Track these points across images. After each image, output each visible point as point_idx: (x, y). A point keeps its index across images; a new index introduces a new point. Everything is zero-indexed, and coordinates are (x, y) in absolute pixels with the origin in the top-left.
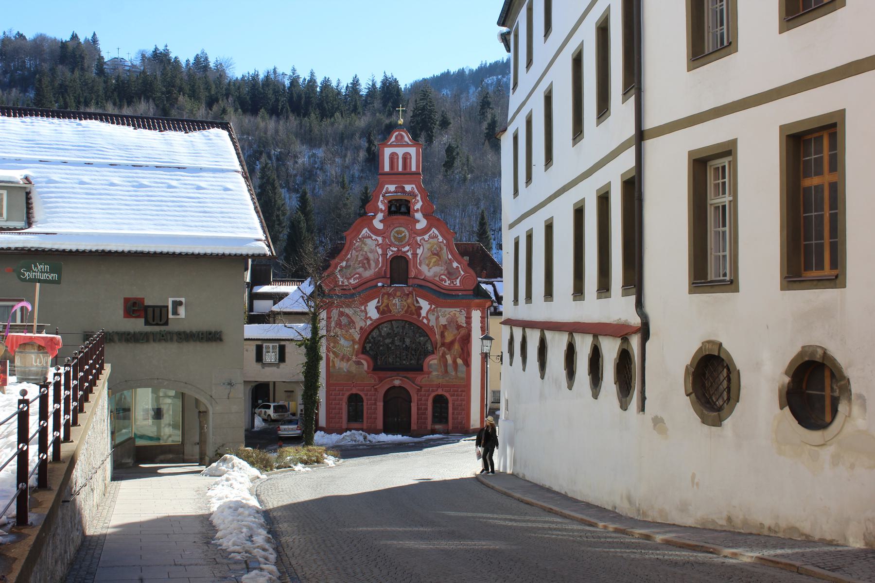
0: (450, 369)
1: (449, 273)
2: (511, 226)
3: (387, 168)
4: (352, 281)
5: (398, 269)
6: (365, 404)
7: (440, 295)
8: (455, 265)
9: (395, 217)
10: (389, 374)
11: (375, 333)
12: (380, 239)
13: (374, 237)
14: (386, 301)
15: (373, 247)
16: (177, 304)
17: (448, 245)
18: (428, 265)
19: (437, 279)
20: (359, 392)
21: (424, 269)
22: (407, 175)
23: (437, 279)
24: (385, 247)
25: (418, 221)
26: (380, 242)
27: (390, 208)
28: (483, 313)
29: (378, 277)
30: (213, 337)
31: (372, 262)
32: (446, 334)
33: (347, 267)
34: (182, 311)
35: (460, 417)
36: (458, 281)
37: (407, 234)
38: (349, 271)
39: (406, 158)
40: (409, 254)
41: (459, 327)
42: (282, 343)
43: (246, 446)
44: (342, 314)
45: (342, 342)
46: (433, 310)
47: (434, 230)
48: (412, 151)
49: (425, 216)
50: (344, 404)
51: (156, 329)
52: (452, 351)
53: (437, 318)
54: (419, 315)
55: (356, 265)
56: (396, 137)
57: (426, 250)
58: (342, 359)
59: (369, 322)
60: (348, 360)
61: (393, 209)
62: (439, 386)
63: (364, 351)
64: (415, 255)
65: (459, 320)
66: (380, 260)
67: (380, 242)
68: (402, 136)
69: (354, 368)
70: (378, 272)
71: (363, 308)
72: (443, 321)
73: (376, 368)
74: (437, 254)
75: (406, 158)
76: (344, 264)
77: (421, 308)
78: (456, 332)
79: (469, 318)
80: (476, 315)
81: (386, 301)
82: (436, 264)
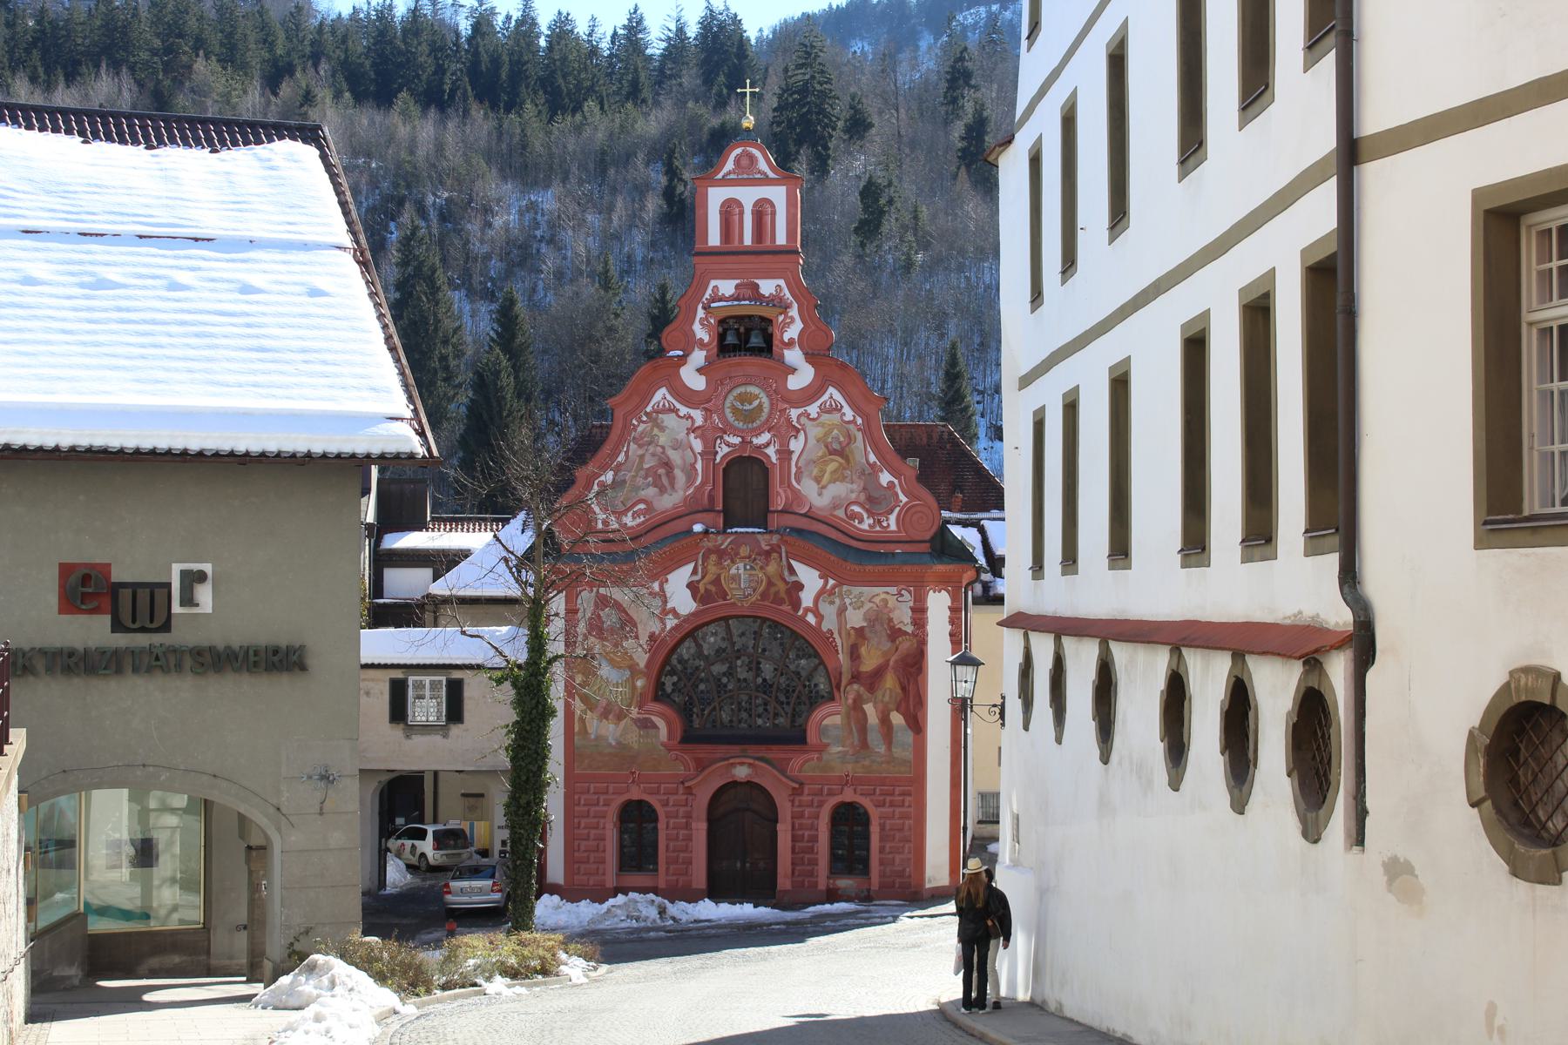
0: (874, 738)
1: (870, 499)
2: (1026, 381)
3: (714, 239)
4: (629, 520)
5: (744, 491)
6: (661, 825)
7: (849, 555)
8: (885, 478)
9: (736, 360)
10: (722, 750)
11: (686, 650)
13: (683, 410)
14: (712, 569)
15: (682, 435)
16: (192, 579)
17: (867, 430)
18: (818, 480)
19: (840, 513)
21: (808, 488)
22: (765, 254)
23: (840, 513)
24: (710, 436)
25: (793, 370)
26: (699, 421)
27: (722, 337)
28: (954, 598)
29: (692, 509)
30: (283, 660)
32: (863, 650)
33: (616, 484)
34: (205, 596)
35: (898, 858)
37: (765, 400)
38: (621, 495)
39: (762, 211)
41: (895, 634)
42: (456, 675)
43: (366, 933)
44: (603, 602)
45: (605, 671)
46: (831, 593)
47: (831, 390)
48: (777, 195)
49: (810, 357)
51: (142, 640)
52: (879, 694)
53: (842, 611)
54: (796, 604)
55: (640, 481)
57: (812, 442)
58: (605, 715)
59: (671, 622)
60: (620, 716)
62: (845, 781)
63: (659, 694)
64: (785, 454)
65: (895, 616)
66: (699, 466)
67: (699, 421)
69: (634, 738)
72: (855, 619)
73: (689, 738)
75: (762, 211)
76: (608, 477)
77: (799, 586)
78: (887, 645)
79: (919, 612)
80: (938, 604)
81: (712, 569)
82: (838, 477)
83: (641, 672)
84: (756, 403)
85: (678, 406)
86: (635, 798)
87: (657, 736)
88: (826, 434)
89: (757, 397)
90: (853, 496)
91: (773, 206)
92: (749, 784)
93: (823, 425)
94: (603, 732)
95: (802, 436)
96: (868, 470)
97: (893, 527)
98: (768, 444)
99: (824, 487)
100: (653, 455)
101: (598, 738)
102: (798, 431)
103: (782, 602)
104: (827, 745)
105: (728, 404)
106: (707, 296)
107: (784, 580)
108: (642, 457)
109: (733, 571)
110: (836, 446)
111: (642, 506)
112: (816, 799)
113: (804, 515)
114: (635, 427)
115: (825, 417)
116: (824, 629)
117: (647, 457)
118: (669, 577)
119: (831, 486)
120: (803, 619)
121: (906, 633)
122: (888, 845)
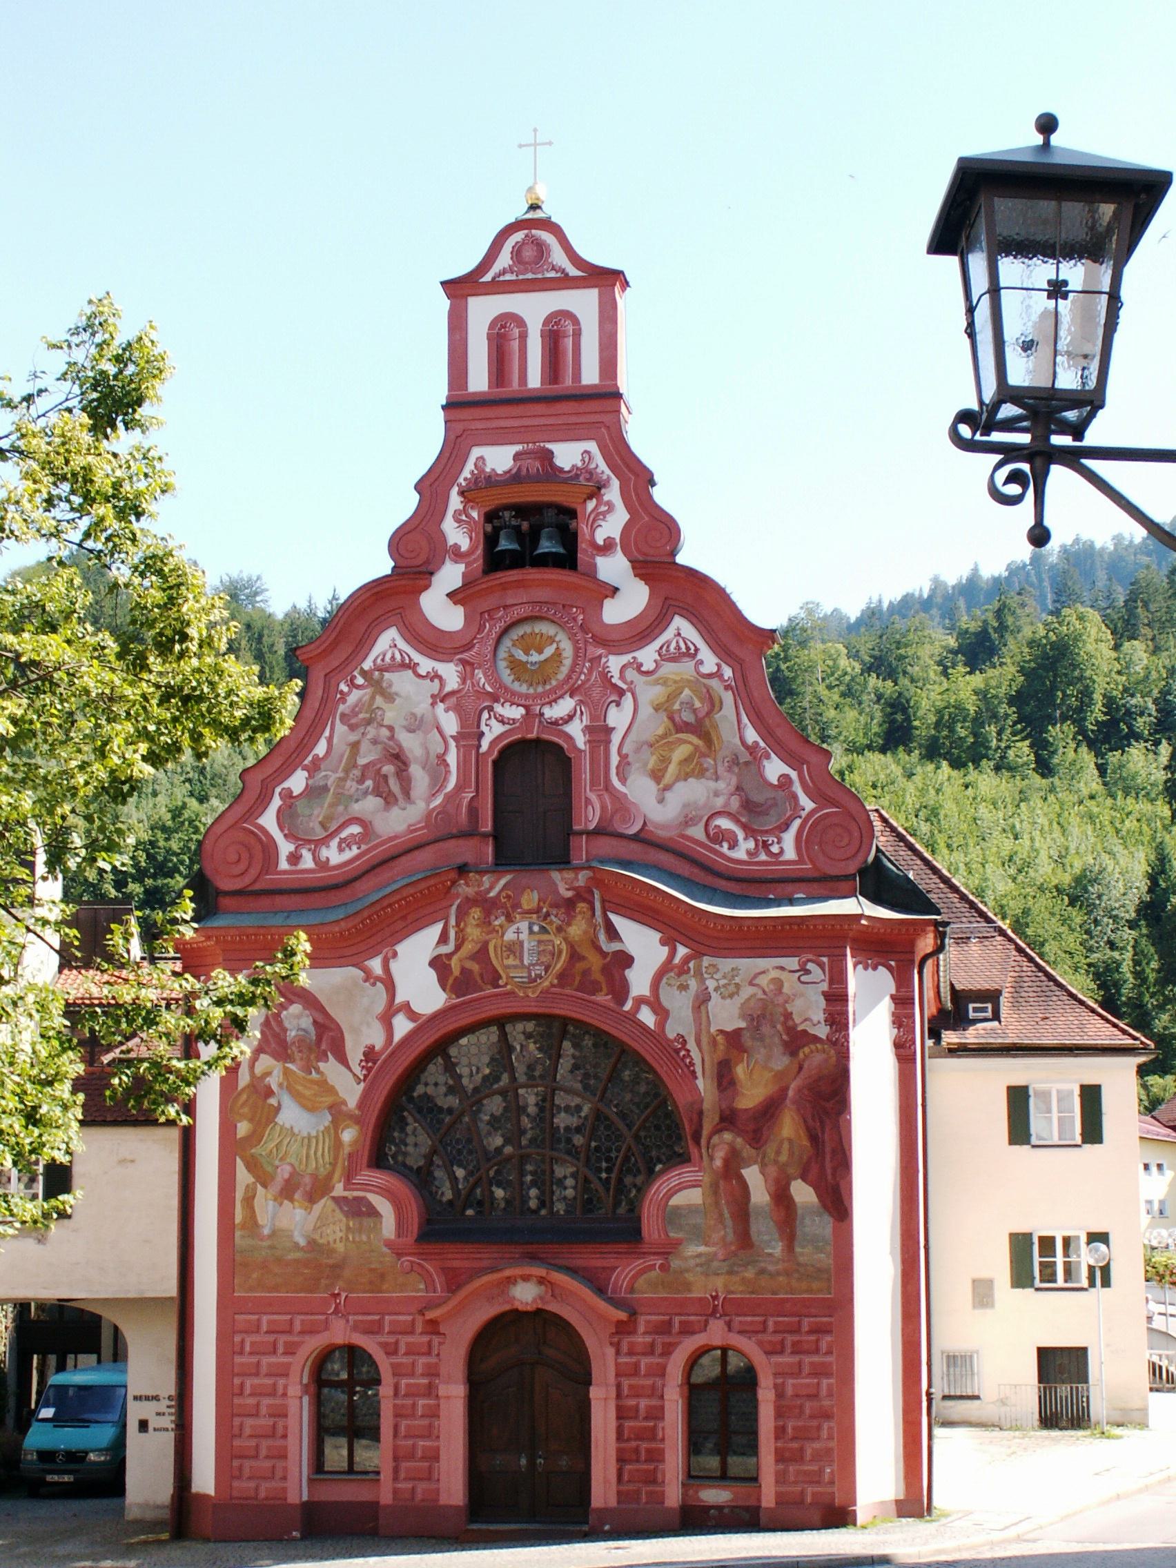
0: (764, 1231)
1: (749, 806)
4: (334, 855)
6: (385, 1390)
7: (702, 891)
8: (774, 769)
9: (513, 575)
12: (450, 673)
13: (426, 665)
14: (474, 933)
15: (423, 707)
18: (657, 776)
19: (697, 832)
20: (360, 1340)
21: (640, 791)
23: (697, 832)
24: (470, 708)
26: (452, 683)
27: (491, 541)
31: (416, 771)
32: (740, 1071)
33: (311, 792)
36: (789, 838)
37: (567, 647)
38: (319, 813)
39: (558, 333)
40: (576, 730)
41: (796, 1040)
45: (291, 1115)
46: (683, 970)
47: (680, 624)
50: (294, 1390)
52: (770, 1149)
53: (702, 1001)
54: (621, 990)
56: (517, 253)
58: (287, 1192)
59: (402, 1026)
61: (504, 544)
62: (712, 1309)
63: (380, 1153)
64: (600, 733)
65: (796, 1008)
66: (452, 759)
67: (452, 683)
68: (541, 249)
69: (336, 1231)
70: (442, 810)
71: (376, 965)
72: (726, 1015)
74: (701, 729)
76: (297, 782)
77: (626, 960)
78: (781, 1062)
79: (837, 999)
81: (474, 933)
82: (693, 769)
83: (351, 1117)
84: (549, 651)
85: (417, 657)
86: (340, 1340)
87: (377, 1228)
88: (671, 698)
89: (551, 640)
90: (719, 803)
91: (576, 321)
92: (539, 1315)
93: (664, 682)
94: (283, 1223)
95: (628, 701)
96: (745, 756)
97: (790, 854)
98: (570, 718)
99: (667, 788)
100: (375, 742)
101: (274, 1233)
102: (621, 693)
103: (595, 989)
104: (678, 1243)
105: (502, 653)
106: (466, 473)
107: (598, 949)
108: (355, 746)
109: (510, 935)
110: (688, 717)
111: (355, 829)
112: (660, 1340)
113: (636, 838)
114: (344, 696)
115: (669, 669)
116: (671, 1035)
117: (365, 746)
118: (399, 948)
119: (680, 786)
120: (632, 1017)
121: (816, 1039)
122: (790, 1425)
